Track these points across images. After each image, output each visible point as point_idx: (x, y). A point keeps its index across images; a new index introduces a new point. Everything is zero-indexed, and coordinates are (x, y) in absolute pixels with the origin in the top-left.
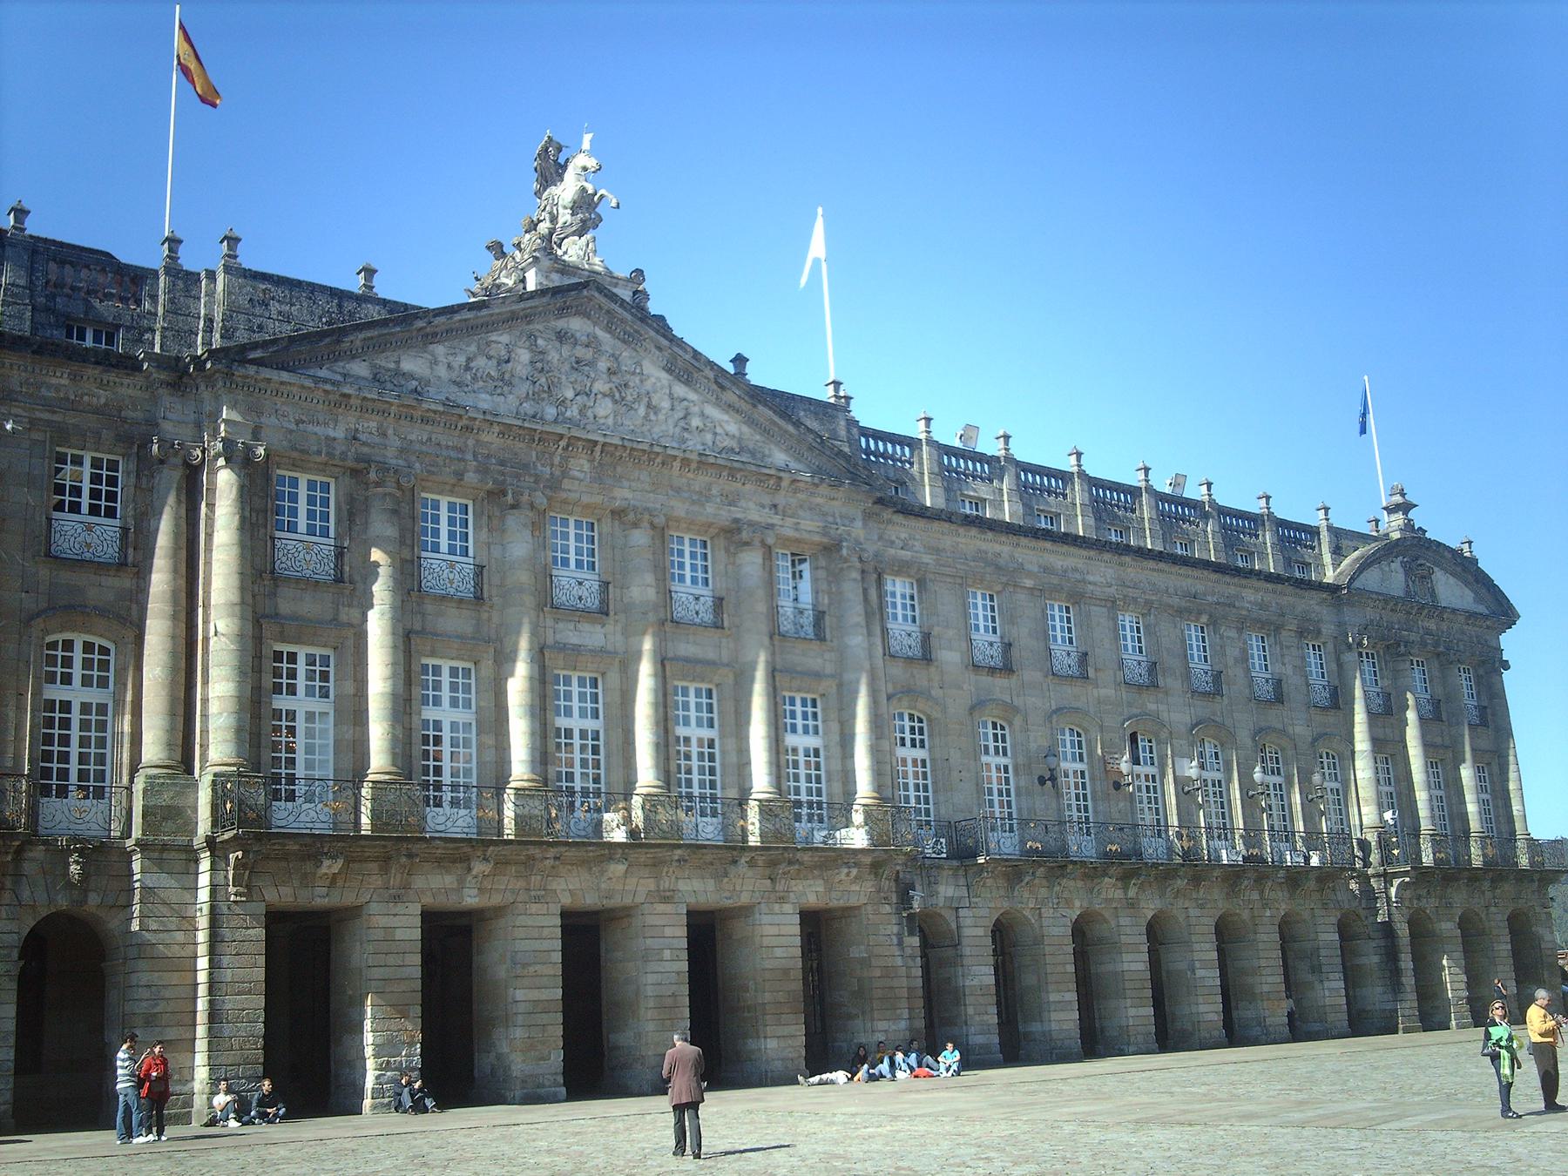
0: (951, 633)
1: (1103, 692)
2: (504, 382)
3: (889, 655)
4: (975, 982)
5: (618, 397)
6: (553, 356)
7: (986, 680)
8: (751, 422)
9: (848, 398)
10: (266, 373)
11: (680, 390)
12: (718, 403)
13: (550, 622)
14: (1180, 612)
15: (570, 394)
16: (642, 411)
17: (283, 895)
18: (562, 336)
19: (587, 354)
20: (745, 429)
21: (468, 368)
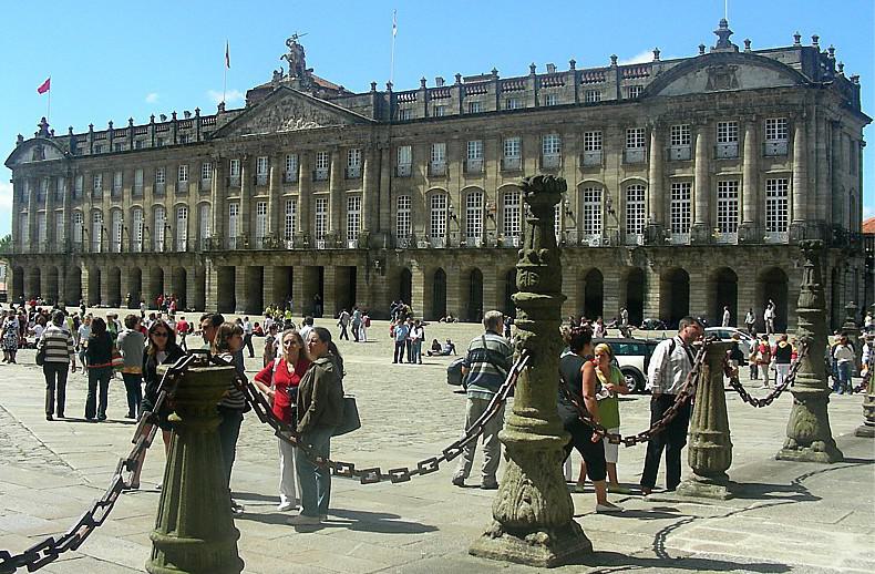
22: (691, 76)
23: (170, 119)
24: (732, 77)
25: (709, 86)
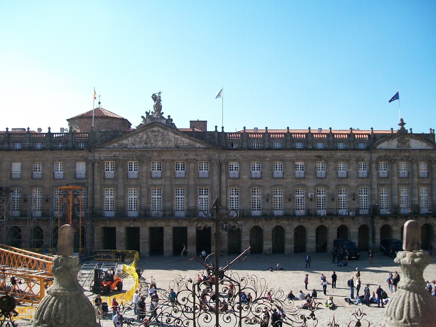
0: (246, 172)
1: (288, 180)
2: (141, 142)
3: (228, 177)
4: (245, 239)
5: (163, 140)
6: (151, 136)
7: (254, 181)
8: (191, 140)
9: (223, 128)
10: (99, 149)
11: (176, 136)
12: (184, 137)
13: (151, 181)
14: (315, 160)
15: (153, 142)
16: (168, 142)
17: (104, 225)
18: (153, 131)
19: (157, 134)
20: (191, 141)
21: (135, 140)
22: (390, 141)
23: (46, 131)
24: (408, 143)
25: (398, 146)
